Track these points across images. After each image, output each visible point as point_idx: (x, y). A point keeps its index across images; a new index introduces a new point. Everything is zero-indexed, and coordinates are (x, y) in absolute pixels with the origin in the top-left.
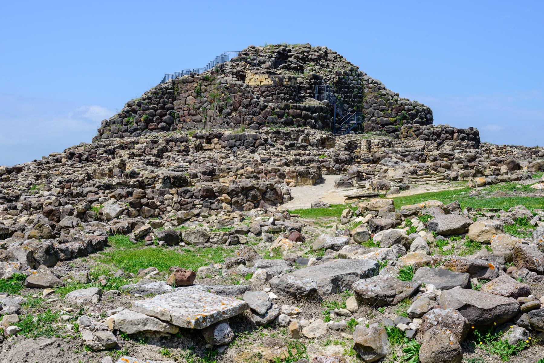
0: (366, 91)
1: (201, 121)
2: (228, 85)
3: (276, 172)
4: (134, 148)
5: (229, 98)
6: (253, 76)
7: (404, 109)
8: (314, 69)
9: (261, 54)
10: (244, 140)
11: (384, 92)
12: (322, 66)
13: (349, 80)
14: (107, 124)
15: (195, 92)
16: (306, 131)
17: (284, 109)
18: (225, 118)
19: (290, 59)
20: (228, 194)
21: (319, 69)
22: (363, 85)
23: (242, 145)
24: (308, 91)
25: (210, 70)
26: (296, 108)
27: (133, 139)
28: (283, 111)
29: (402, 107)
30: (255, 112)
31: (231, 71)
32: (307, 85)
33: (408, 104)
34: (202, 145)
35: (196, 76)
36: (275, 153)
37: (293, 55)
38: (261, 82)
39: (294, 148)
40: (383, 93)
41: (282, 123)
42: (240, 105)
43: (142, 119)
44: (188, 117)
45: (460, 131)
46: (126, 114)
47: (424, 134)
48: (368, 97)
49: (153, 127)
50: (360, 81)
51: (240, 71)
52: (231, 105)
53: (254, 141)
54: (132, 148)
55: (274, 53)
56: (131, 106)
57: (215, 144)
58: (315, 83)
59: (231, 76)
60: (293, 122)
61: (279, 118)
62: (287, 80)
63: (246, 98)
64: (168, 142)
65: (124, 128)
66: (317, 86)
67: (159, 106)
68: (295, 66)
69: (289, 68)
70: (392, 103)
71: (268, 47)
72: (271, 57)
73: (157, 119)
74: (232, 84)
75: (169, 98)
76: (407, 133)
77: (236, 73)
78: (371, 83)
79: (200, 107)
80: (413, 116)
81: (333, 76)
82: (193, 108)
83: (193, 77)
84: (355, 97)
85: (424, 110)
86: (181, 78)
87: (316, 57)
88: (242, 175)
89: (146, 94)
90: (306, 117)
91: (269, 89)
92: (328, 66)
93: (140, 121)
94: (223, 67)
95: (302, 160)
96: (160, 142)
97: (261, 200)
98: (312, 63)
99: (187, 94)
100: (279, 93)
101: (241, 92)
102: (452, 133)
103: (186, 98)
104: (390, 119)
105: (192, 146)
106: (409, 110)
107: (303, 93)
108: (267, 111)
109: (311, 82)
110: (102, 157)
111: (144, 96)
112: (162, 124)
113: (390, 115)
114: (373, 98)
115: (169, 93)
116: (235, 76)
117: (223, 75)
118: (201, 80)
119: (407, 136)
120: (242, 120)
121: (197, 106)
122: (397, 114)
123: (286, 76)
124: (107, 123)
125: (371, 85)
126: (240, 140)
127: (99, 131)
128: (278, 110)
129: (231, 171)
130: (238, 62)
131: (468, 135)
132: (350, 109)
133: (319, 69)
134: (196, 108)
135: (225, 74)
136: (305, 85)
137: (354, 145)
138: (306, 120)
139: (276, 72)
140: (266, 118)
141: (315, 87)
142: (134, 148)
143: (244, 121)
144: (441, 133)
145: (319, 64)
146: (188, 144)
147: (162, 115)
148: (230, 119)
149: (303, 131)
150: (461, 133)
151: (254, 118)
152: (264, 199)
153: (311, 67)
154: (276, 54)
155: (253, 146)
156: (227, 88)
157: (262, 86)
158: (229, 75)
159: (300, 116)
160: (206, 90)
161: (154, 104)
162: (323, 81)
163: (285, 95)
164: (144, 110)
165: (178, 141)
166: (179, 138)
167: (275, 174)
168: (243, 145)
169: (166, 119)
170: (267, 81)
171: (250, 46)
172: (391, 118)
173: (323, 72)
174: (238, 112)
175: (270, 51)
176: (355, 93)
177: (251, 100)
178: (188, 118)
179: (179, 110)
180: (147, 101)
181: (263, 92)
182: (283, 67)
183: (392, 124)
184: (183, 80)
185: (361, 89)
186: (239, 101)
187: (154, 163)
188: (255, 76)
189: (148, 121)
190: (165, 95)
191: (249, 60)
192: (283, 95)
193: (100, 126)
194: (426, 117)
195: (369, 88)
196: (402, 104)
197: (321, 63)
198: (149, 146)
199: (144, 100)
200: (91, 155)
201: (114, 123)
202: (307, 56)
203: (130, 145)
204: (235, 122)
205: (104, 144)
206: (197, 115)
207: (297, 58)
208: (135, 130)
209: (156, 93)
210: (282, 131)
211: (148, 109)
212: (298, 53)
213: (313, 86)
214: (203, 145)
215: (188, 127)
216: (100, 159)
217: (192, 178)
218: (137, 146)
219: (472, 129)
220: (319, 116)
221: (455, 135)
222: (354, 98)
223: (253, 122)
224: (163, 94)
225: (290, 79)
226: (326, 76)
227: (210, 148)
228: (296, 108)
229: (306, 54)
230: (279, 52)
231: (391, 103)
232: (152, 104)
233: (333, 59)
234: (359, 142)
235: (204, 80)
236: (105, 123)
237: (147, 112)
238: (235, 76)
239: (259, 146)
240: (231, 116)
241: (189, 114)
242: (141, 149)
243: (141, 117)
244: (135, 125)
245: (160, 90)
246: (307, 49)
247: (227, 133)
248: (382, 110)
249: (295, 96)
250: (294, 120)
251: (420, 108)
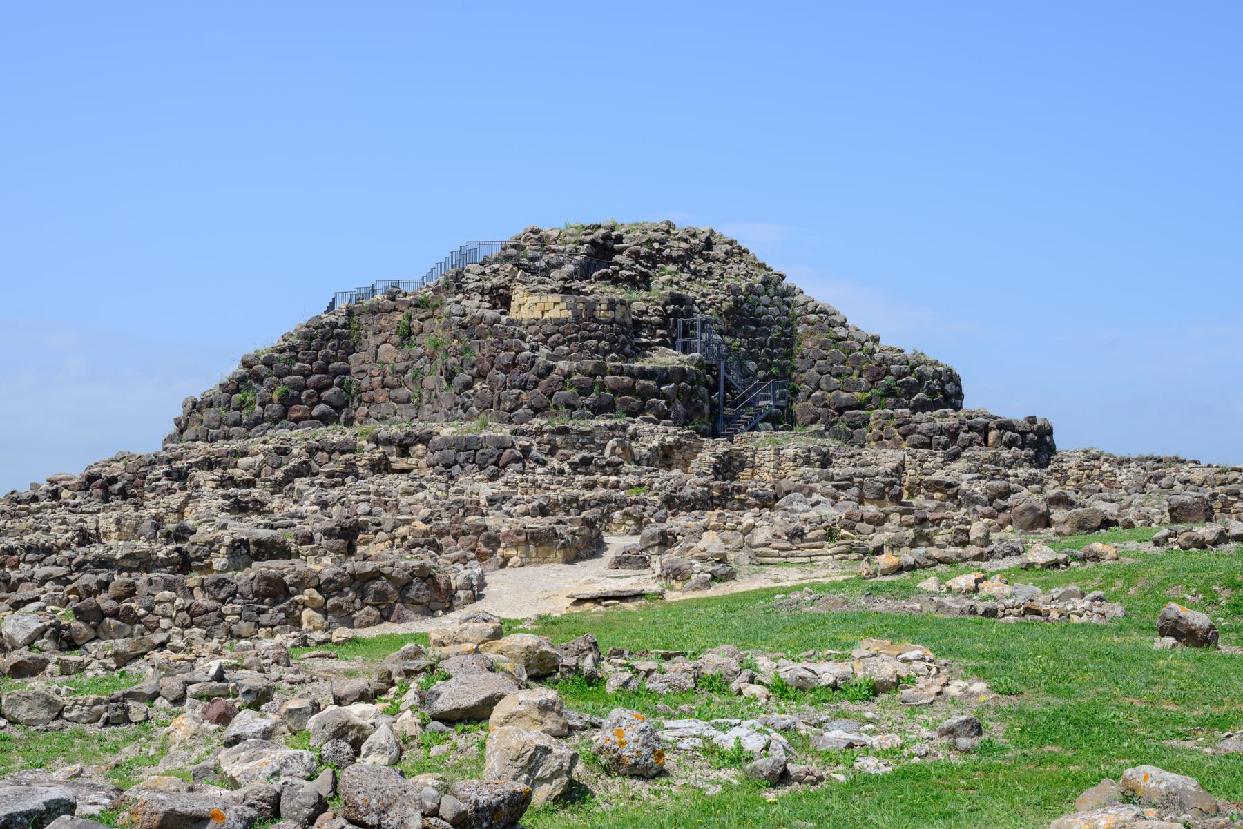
0: (800, 330)
1: (409, 401)
2: (466, 320)
3: (478, 533)
4: (236, 466)
5: (468, 349)
6: (526, 298)
7: (888, 373)
8: (675, 279)
9: (553, 247)
10: (476, 451)
11: (842, 332)
12: (695, 273)
13: (759, 305)
14: (195, 407)
15: (396, 333)
16: (631, 427)
17: (594, 376)
18: (458, 394)
19: (617, 258)
20: (318, 588)
21: (689, 279)
22: (795, 318)
23: (471, 461)
24: (660, 332)
25: (432, 284)
26: (621, 372)
27: (236, 444)
28: (591, 380)
29: (884, 366)
30: (526, 382)
31: (479, 287)
32: (656, 319)
33: (899, 360)
34: (387, 459)
35: (400, 297)
36: (537, 481)
37: (626, 248)
38: (543, 312)
39: (592, 468)
40: (839, 334)
41: (588, 406)
42: (492, 365)
43: (275, 396)
44: (380, 391)
45: (1004, 426)
46: (238, 384)
47: (920, 433)
48: (806, 344)
49: (299, 414)
50: (785, 307)
51: (497, 288)
52: (473, 366)
53: (497, 453)
54: (232, 464)
55: (582, 243)
56: (251, 367)
57: (418, 457)
58: (676, 314)
59: (479, 297)
60: (614, 404)
61: (580, 394)
62: (604, 307)
63: (506, 350)
64: (312, 451)
65: (233, 416)
66: (680, 320)
67: (315, 366)
68: (628, 273)
69: (615, 280)
70: (861, 357)
71: (570, 231)
72: (576, 252)
73: (308, 396)
74: (474, 317)
75: (339, 348)
76: (882, 429)
77: (491, 291)
78: (813, 312)
79: (408, 368)
80: (911, 389)
81: (721, 296)
82: (392, 369)
83: (393, 299)
84: (774, 343)
85: (937, 375)
86: (367, 302)
87: (681, 253)
88: (404, 538)
89: (286, 337)
90: (644, 394)
91: (562, 328)
92: (710, 272)
93: (271, 401)
94: (460, 276)
95: (585, 501)
96: (295, 451)
97: (396, 602)
98: (672, 267)
99: (379, 339)
100: (584, 338)
101: (496, 336)
102: (985, 430)
103: (378, 347)
104: (857, 395)
105: (364, 462)
106: (901, 375)
107: (646, 337)
108: (553, 379)
109: (666, 310)
110: (157, 486)
111: (282, 343)
112: (322, 408)
113: (856, 387)
114: (817, 347)
115: (339, 336)
116: (487, 298)
117: (460, 296)
118: (411, 306)
119: (881, 438)
120: (496, 401)
121: (400, 367)
122: (872, 383)
123: (604, 299)
124: (194, 404)
125: (813, 317)
126: (466, 450)
127: (178, 422)
128: (579, 376)
129: (382, 530)
130: (496, 266)
131: (1023, 433)
132: (761, 374)
133: (689, 279)
134: (398, 372)
135: (464, 293)
136: (653, 318)
137: (739, 459)
138: (645, 400)
139: (584, 287)
140: (550, 396)
141: (675, 322)
142: (236, 466)
143: (500, 401)
144: (957, 429)
145: (689, 267)
146: (355, 458)
147: (320, 388)
148: (469, 397)
149: (624, 428)
150: (1007, 430)
151: (524, 396)
152: (403, 600)
153: (668, 277)
154: (586, 245)
155: (496, 464)
156: (464, 327)
157: (545, 322)
158: (473, 294)
159: (630, 390)
160: (421, 331)
161: (303, 361)
162: (696, 308)
163: (599, 342)
164: (280, 377)
165: (334, 451)
166: (339, 444)
167: (475, 537)
168: (474, 462)
169: (330, 395)
170: (558, 310)
171: (529, 227)
172: (860, 394)
173: (696, 287)
174: (487, 380)
175: (573, 239)
176: (774, 336)
177: (518, 353)
178: (381, 395)
179: (362, 376)
180: (287, 354)
181: (548, 336)
182: (603, 277)
183: (860, 406)
184: (371, 306)
185: (788, 325)
186: (490, 356)
187: (250, 505)
188: (530, 298)
189: (288, 401)
190: (328, 340)
191: (524, 261)
192: (594, 342)
193: (179, 413)
194: (943, 391)
195: (809, 324)
196: (884, 361)
197: (692, 267)
198: (270, 462)
199: (282, 351)
200: (133, 481)
201: (211, 405)
202: (659, 251)
203: (227, 459)
204: (480, 404)
205: (168, 455)
206: (400, 386)
207: (636, 256)
208: (259, 420)
209: (307, 337)
210: (575, 427)
211: (289, 373)
212: (637, 245)
213: (671, 319)
214: (391, 459)
215: (379, 416)
216: (153, 490)
217: (301, 545)
218: (243, 461)
219: (1032, 420)
220: (679, 392)
221: (992, 435)
222: (772, 346)
223: (522, 404)
224: (326, 338)
225: (612, 305)
226: (704, 295)
227: (406, 466)
228: (621, 372)
229: (656, 245)
230: (593, 242)
231: (858, 359)
232: (297, 361)
233: (722, 256)
234: (748, 454)
235: (417, 306)
236: (190, 405)
237: (286, 379)
238: (487, 298)
239: (508, 463)
240: (472, 391)
241: (384, 386)
242: (251, 467)
243: (272, 392)
244: (258, 409)
245: (317, 328)
246: (659, 235)
248: (838, 375)
249: (624, 344)
250: (618, 399)
251: (929, 370)
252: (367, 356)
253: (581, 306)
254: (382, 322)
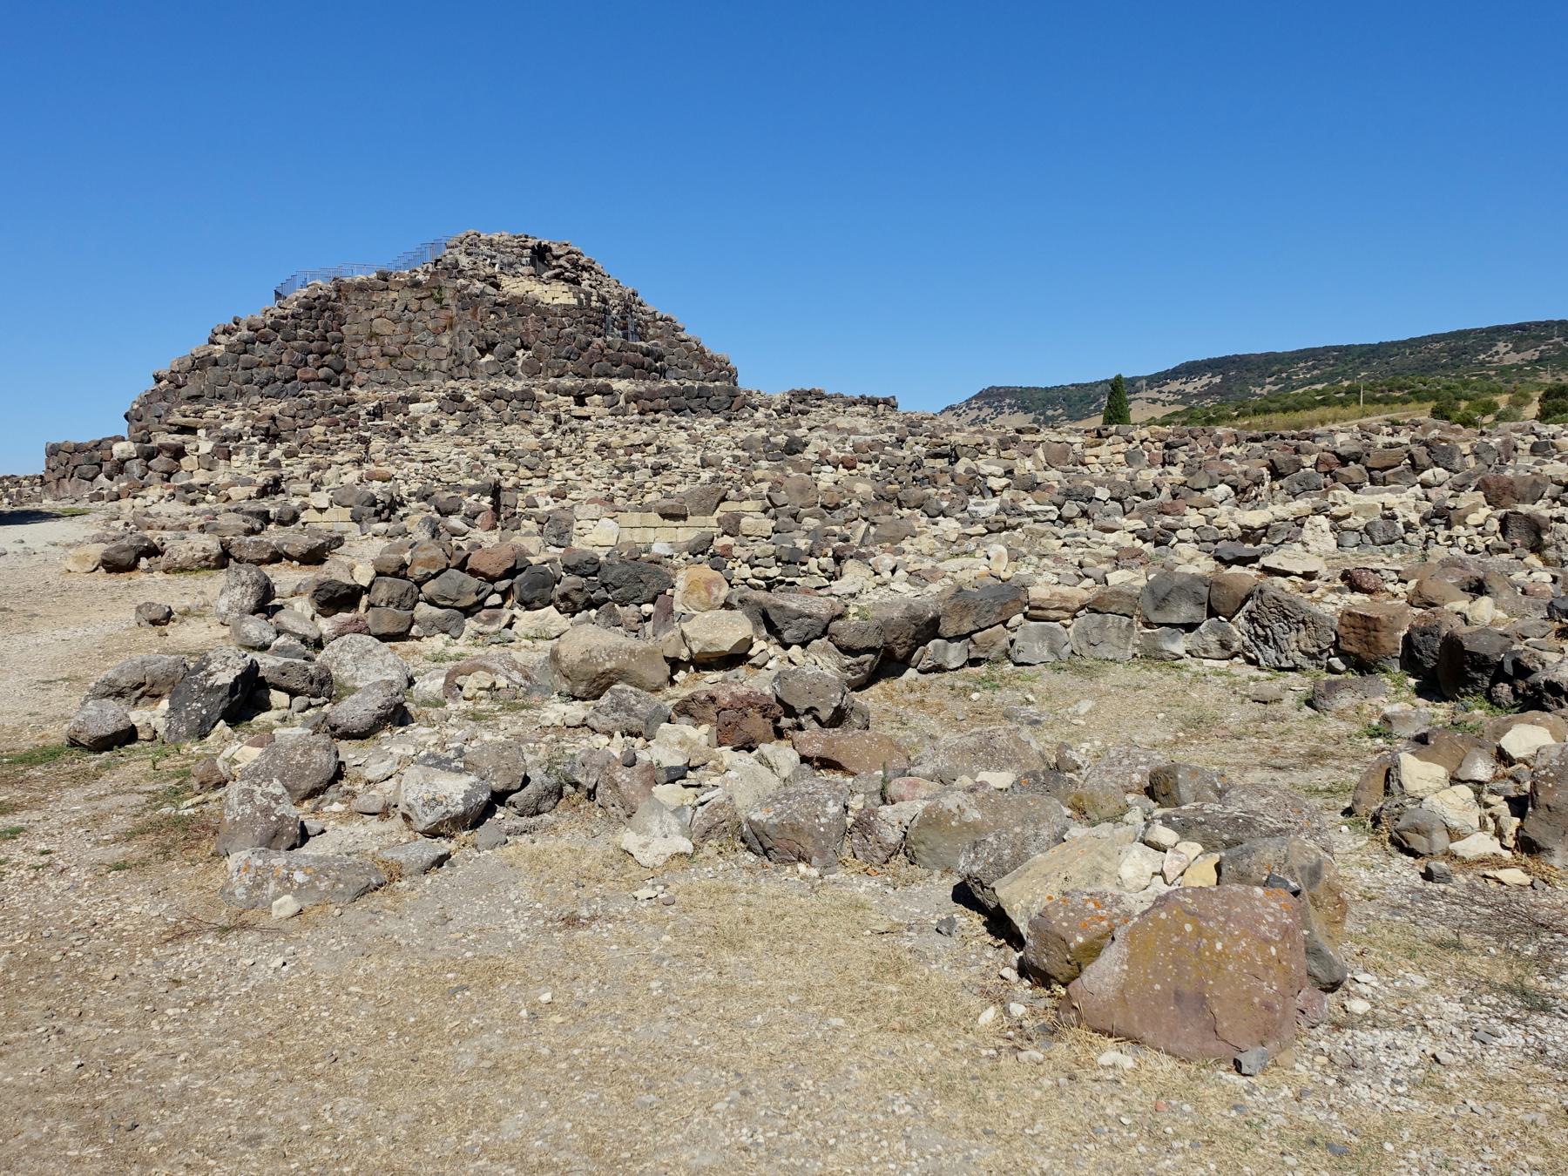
11: (684, 337)
49: (309, 375)
55: (524, 248)
73: (315, 360)
83: (386, 280)
96: (468, 398)
98: (586, 275)
99: (373, 314)
103: (372, 320)
112: (322, 373)
117: (461, 281)
125: (660, 323)
135: (464, 278)
140: (591, 366)
156: (502, 305)
171: (473, 231)
179: (355, 345)
199: (285, 318)
201: (216, 363)
216: (368, 430)
227: (585, 414)
237: (295, 344)
245: (315, 300)
247: (618, 385)
252: (363, 330)
254: (374, 298)
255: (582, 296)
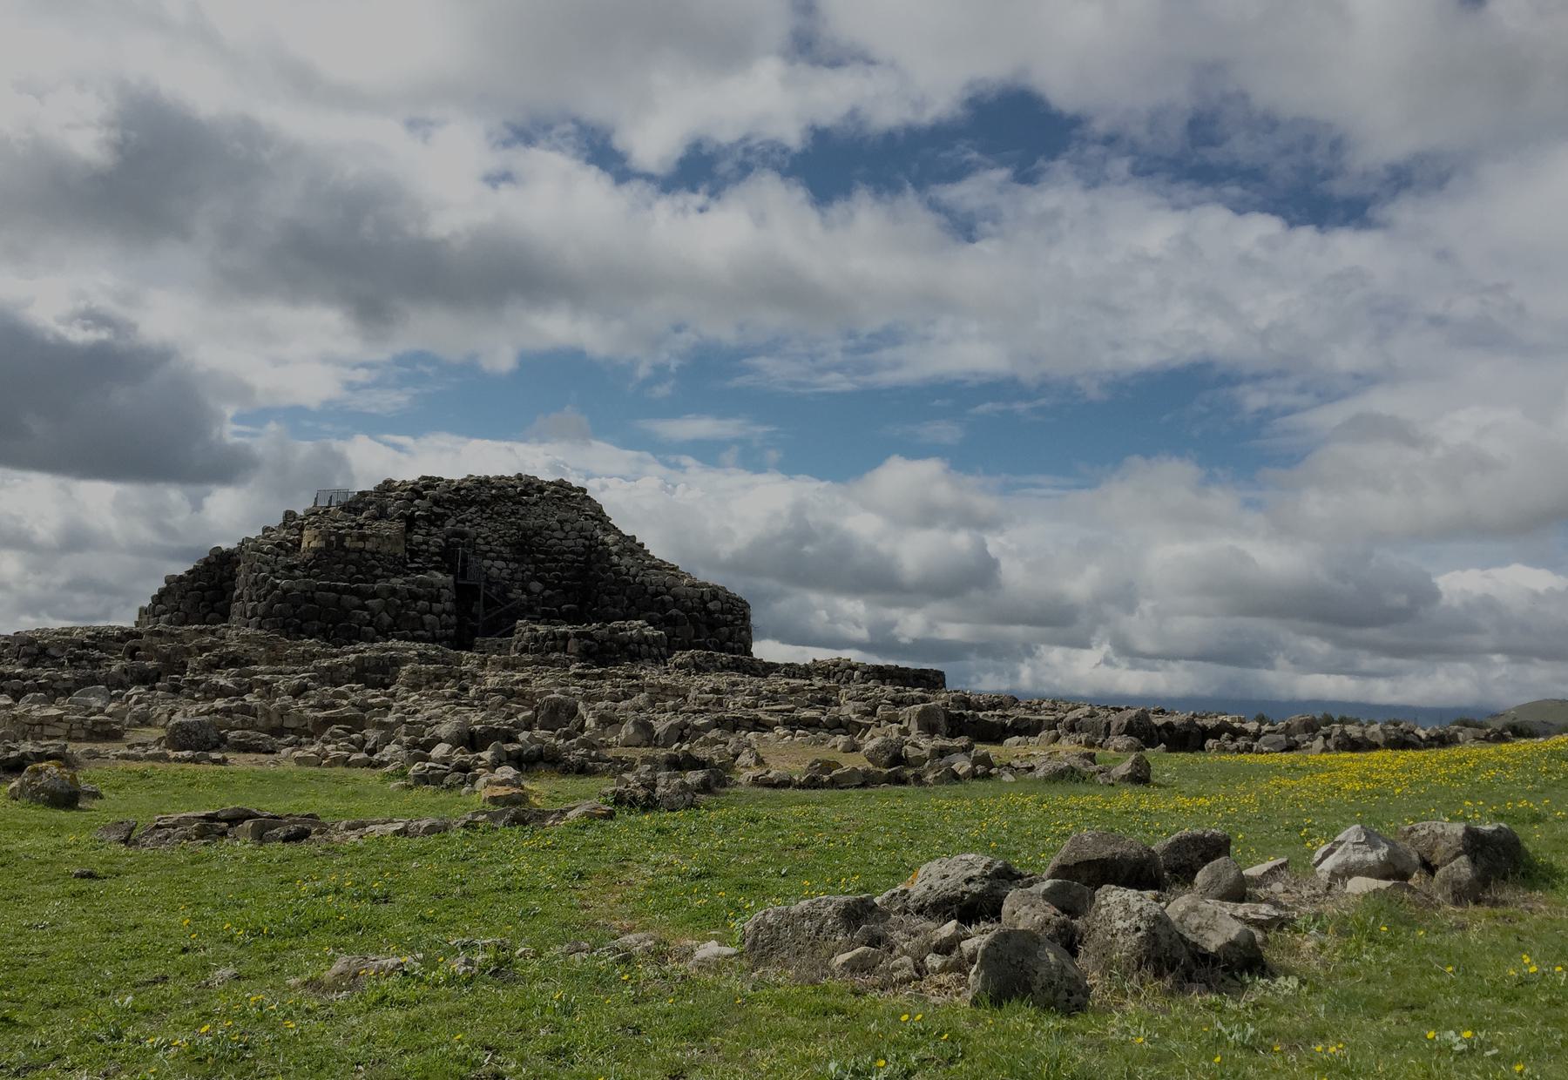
194: (705, 608)
229: (462, 492)
253: (333, 538)
255: (333, 538)
